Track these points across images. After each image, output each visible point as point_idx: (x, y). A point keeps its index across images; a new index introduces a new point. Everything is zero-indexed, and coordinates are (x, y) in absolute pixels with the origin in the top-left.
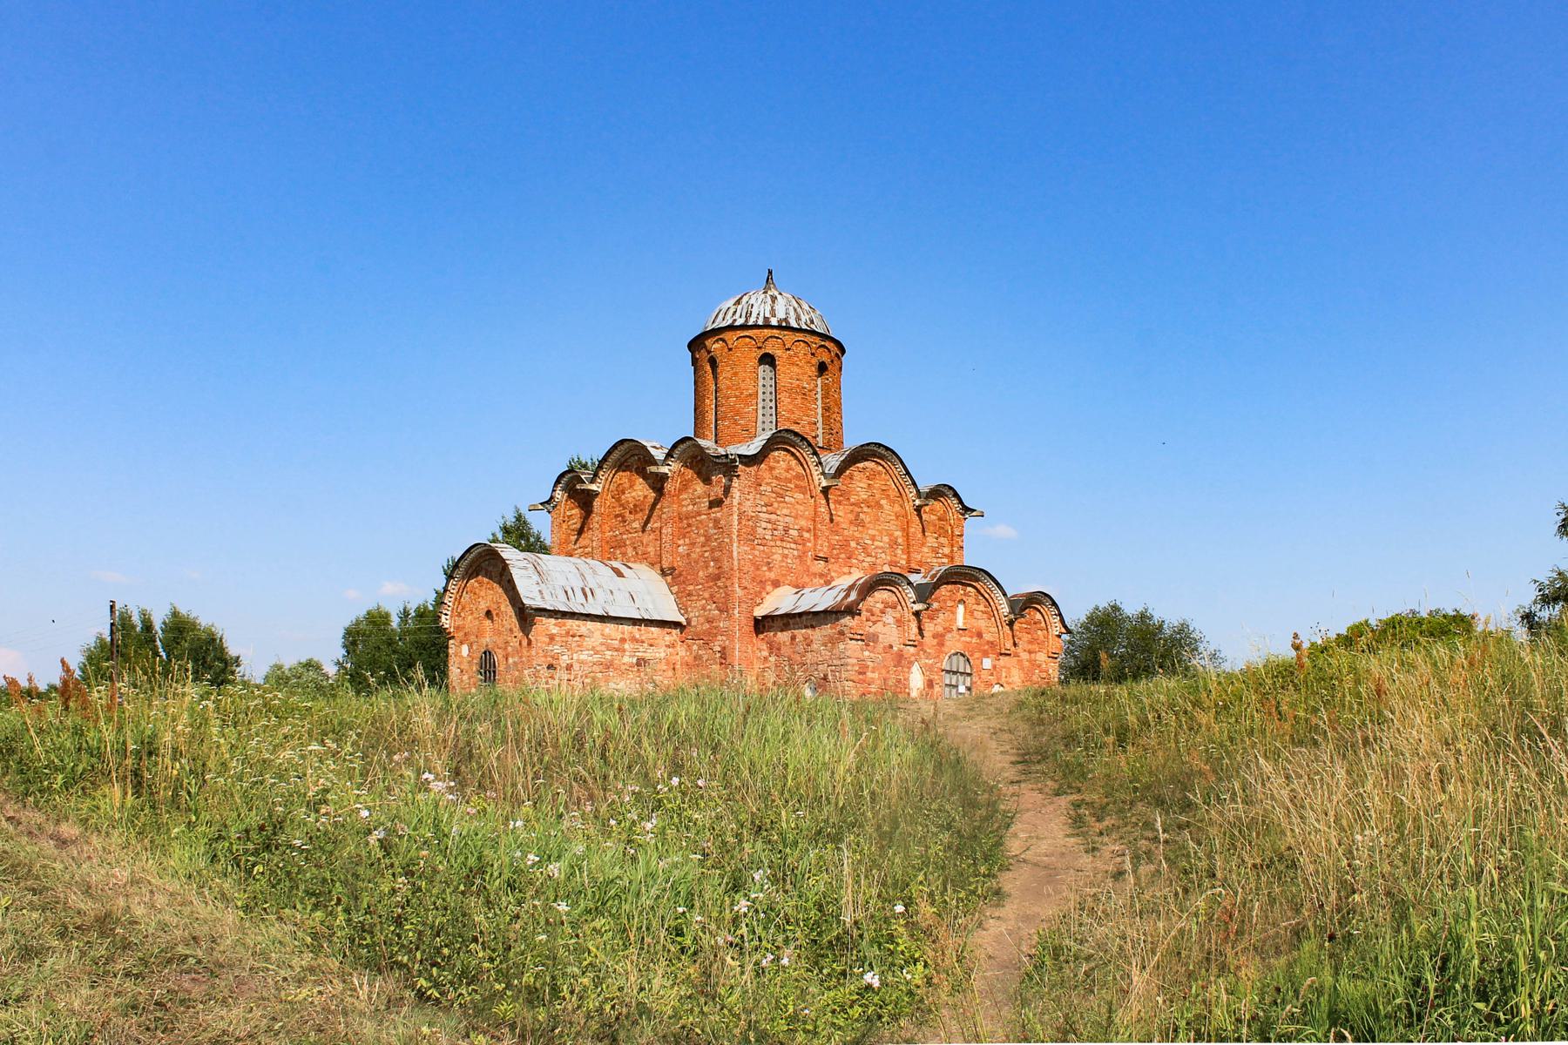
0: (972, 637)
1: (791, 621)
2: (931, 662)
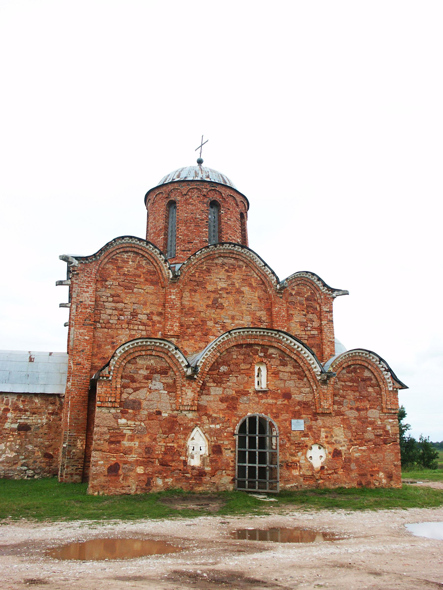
0: (276, 399)
2: (218, 426)
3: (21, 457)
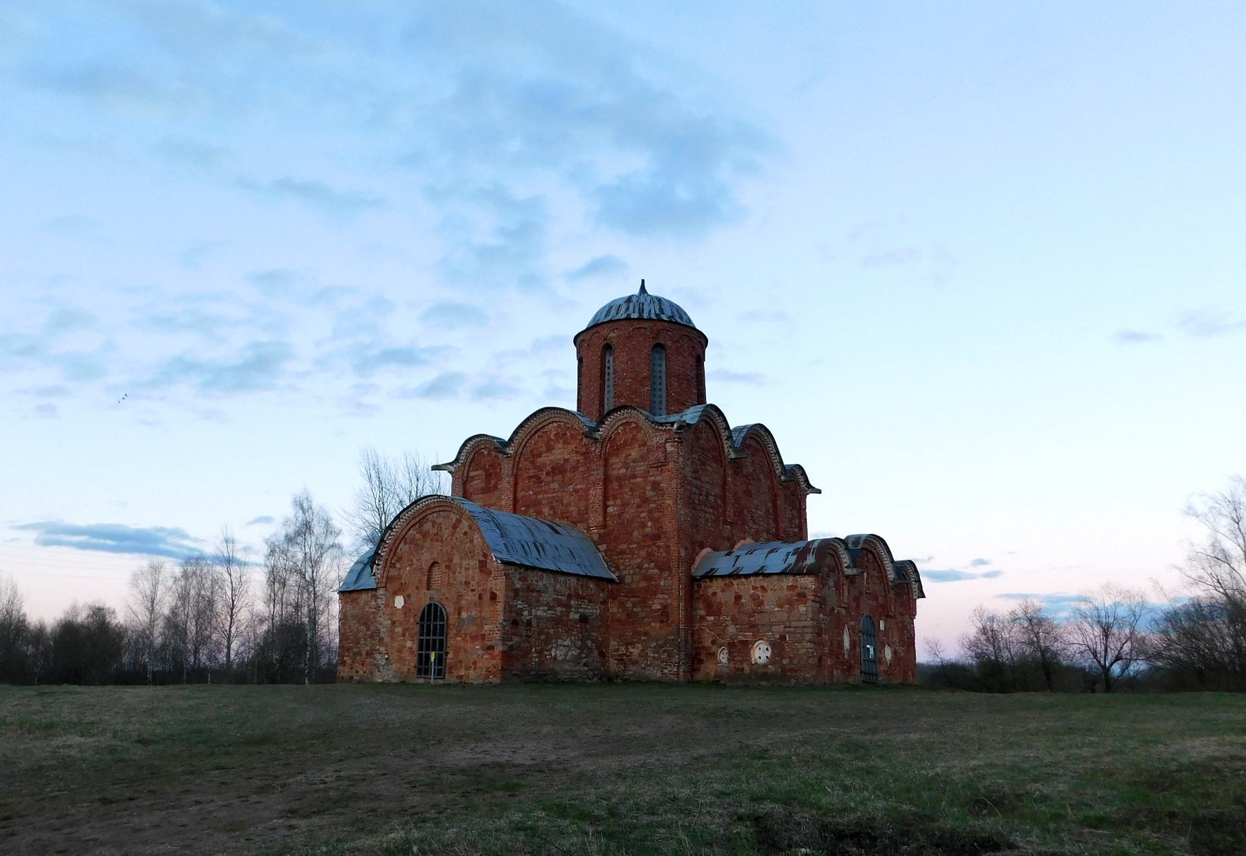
1: (735, 582)
3: (583, 655)
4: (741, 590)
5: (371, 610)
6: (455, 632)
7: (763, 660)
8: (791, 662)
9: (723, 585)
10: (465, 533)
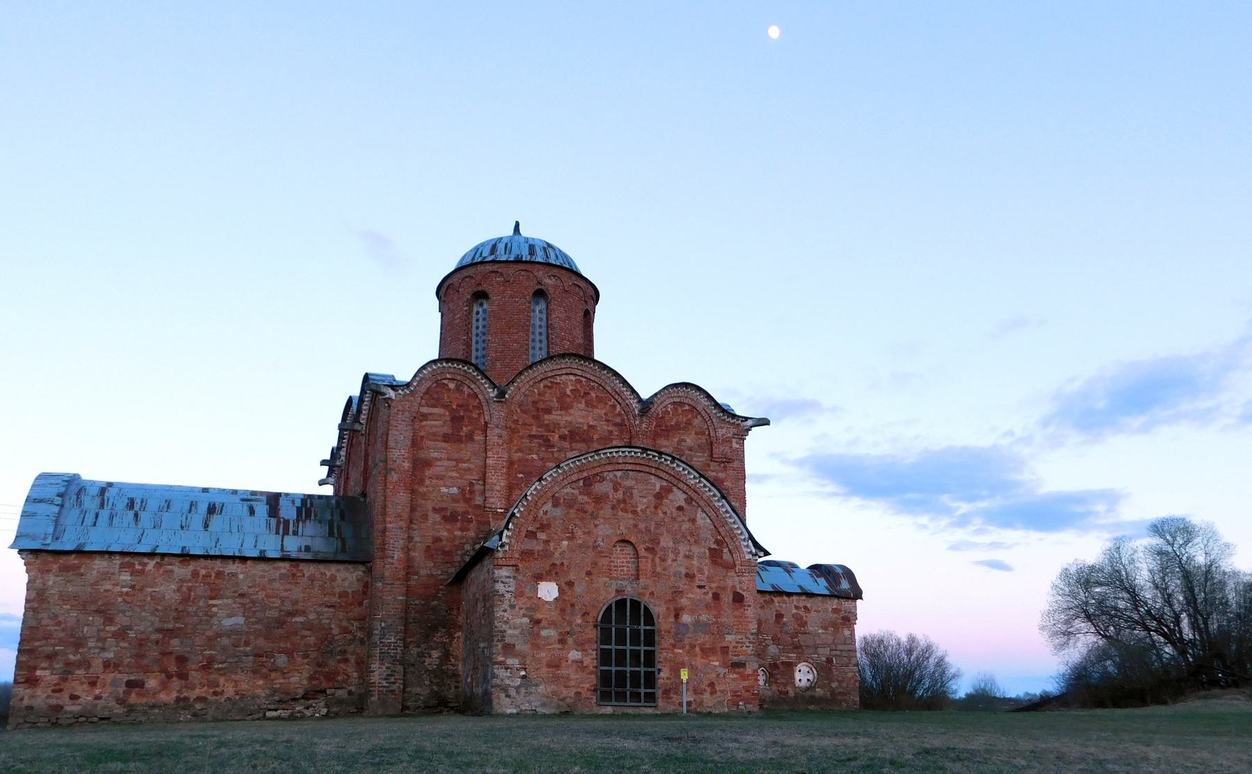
1: (776, 600)
4: (782, 607)
5: (118, 589)
6: (672, 641)
7: (804, 683)
8: (840, 686)
9: (762, 601)
10: (680, 508)
